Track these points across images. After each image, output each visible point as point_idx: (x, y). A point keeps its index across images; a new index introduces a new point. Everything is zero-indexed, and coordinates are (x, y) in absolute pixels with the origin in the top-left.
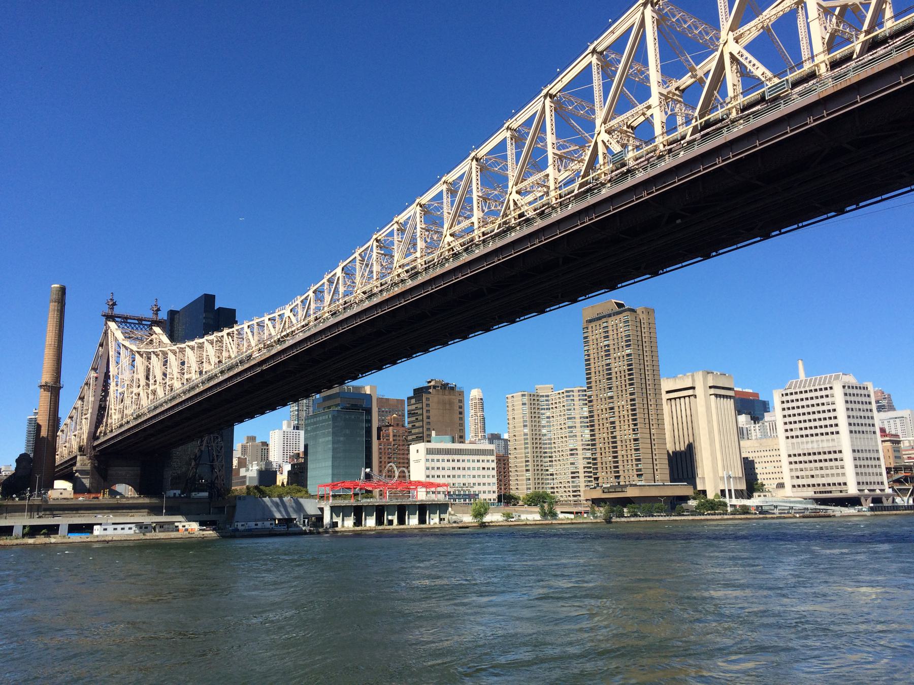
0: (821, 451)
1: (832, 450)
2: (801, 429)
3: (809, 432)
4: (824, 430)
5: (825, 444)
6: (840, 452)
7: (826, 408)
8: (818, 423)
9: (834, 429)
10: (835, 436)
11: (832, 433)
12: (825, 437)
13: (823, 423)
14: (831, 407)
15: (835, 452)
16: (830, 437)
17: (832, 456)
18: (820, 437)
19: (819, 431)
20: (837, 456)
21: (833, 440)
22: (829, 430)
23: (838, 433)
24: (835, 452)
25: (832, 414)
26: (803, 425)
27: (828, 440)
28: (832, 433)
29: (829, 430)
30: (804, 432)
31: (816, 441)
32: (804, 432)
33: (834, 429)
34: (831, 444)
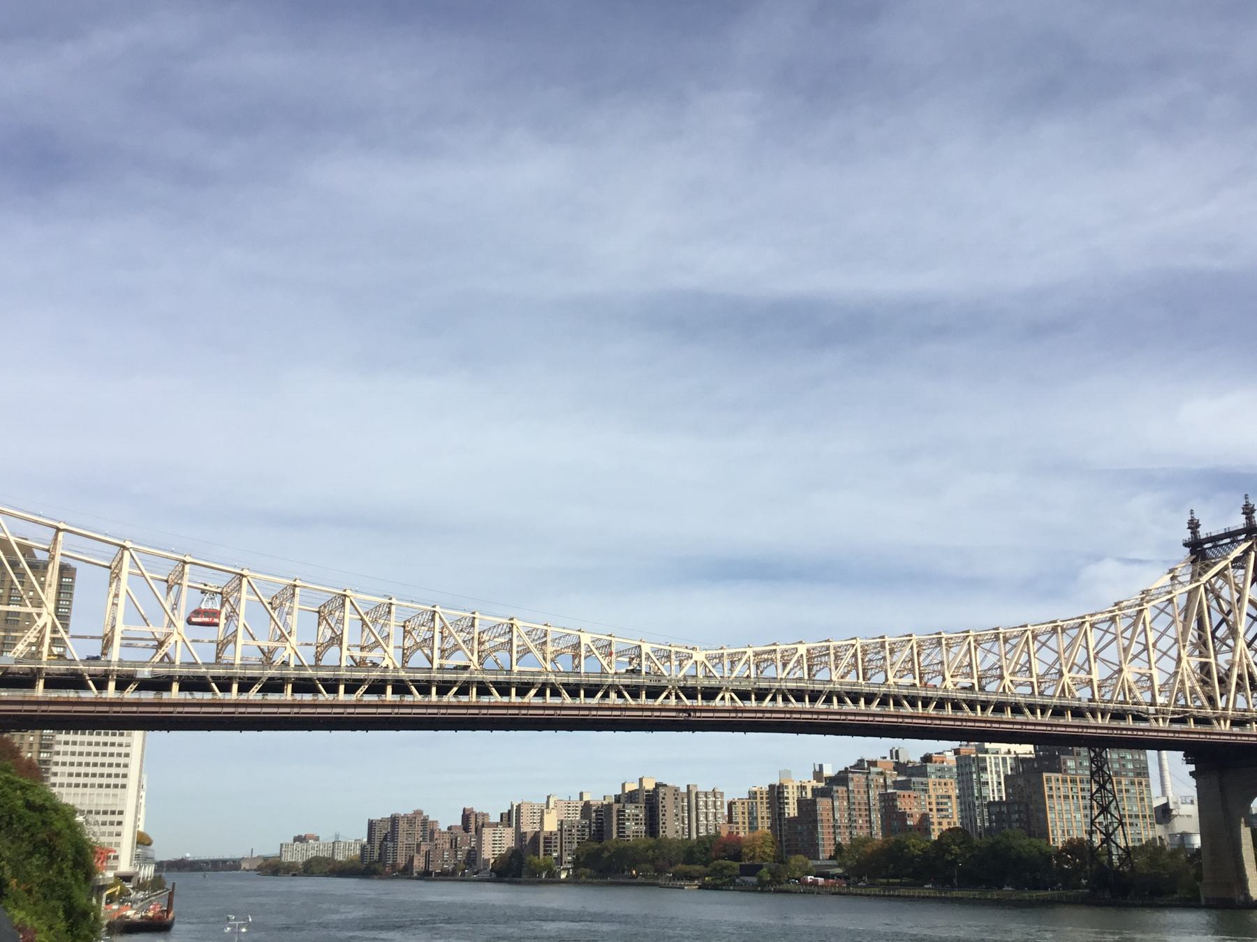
0: (94, 809)
1: (109, 809)
2: (70, 775)
3: (81, 780)
4: (105, 781)
5: (103, 801)
6: (121, 813)
7: (115, 750)
8: (98, 770)
9: (120, 781)
10: (119, 791)
11: (116, 786)
12: (104, 790)
13: (106, 770)
14: (123, 750)
15: (113, 813)
16: (111, 791)
17: (109, 818)
18: (97, 790)
19: (97, 781)
20: (116, 818)
21: (115, 795)
22: (112, 781)
23: (124, 786)
24: (113, 813)
25: (122, 760)
26: (75, 770)
27: (107, 795)
28: (116, 786)
29: (112, 781)
30: (74, 780)
31: (90, 794)
32: (74, 780)
33: (120, 781)
34: (111, 801)
